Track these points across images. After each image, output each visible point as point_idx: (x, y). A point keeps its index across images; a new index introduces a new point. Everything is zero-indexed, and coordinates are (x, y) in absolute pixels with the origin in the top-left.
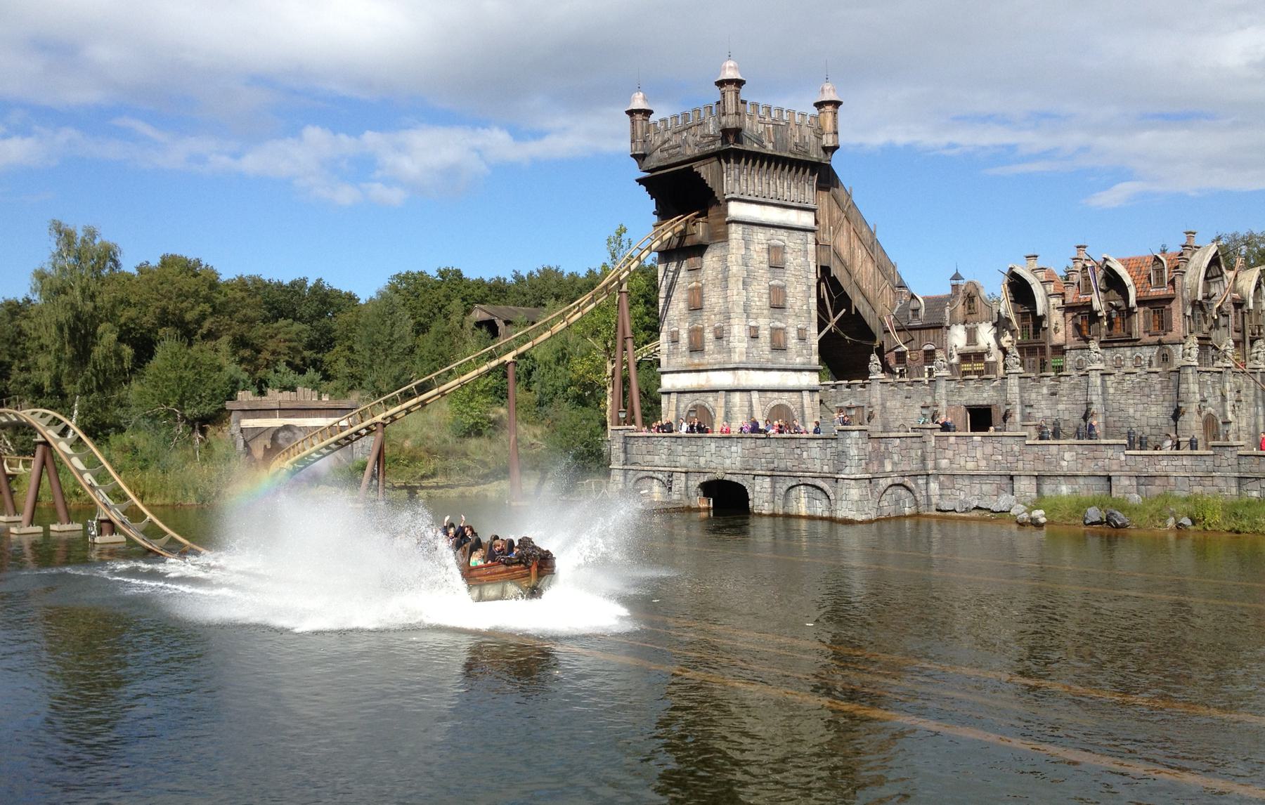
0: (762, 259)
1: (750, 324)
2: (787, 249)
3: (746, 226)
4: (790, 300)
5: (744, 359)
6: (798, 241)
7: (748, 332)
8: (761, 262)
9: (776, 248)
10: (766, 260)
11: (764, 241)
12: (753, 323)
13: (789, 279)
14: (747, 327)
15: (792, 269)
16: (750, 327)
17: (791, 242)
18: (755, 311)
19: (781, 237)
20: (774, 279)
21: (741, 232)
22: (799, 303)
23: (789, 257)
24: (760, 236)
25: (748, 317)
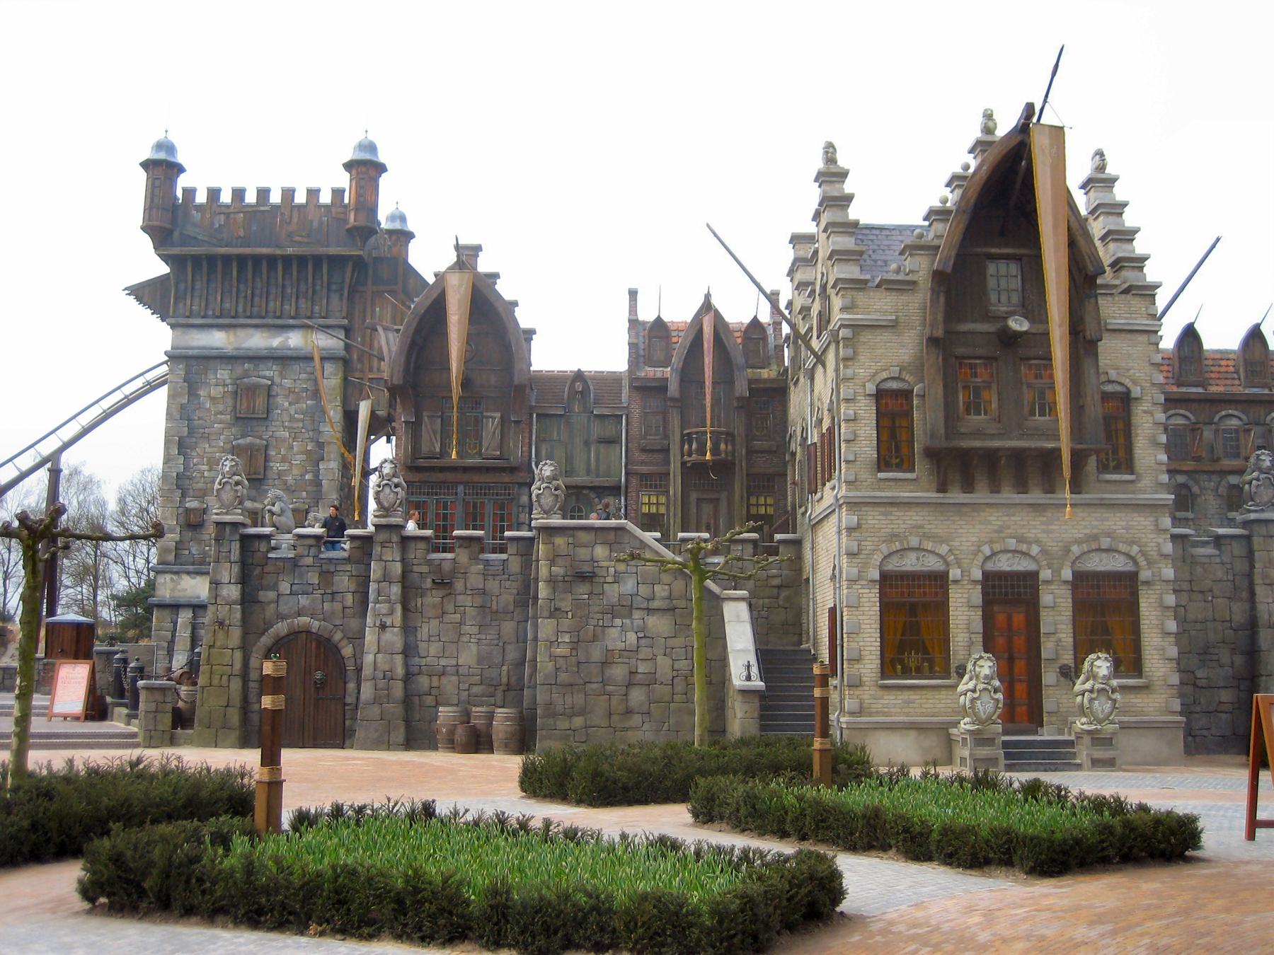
0: (221, 407)
1: (187, 505)
2: (276, 389)
3: (194, 362)
4: (276, 466)
5: (171, 558)
6: (303, 376)
7: (182, 519)
8: (221, 413)
9: (252, 390)
10: (229, 409)
11: (228, 381)
12: (192, 504)
13: (277, 434)
14: (181, 510)
15: (286, 418)
16: (188, 511)
17: (288, 381)
18: (200, 485)
19: (267, 373)
20: (243, 436)
21: (182, 373)
22: (295, 471)
23: (282, 402)
24: (223, 374)
25: (183, 496)
